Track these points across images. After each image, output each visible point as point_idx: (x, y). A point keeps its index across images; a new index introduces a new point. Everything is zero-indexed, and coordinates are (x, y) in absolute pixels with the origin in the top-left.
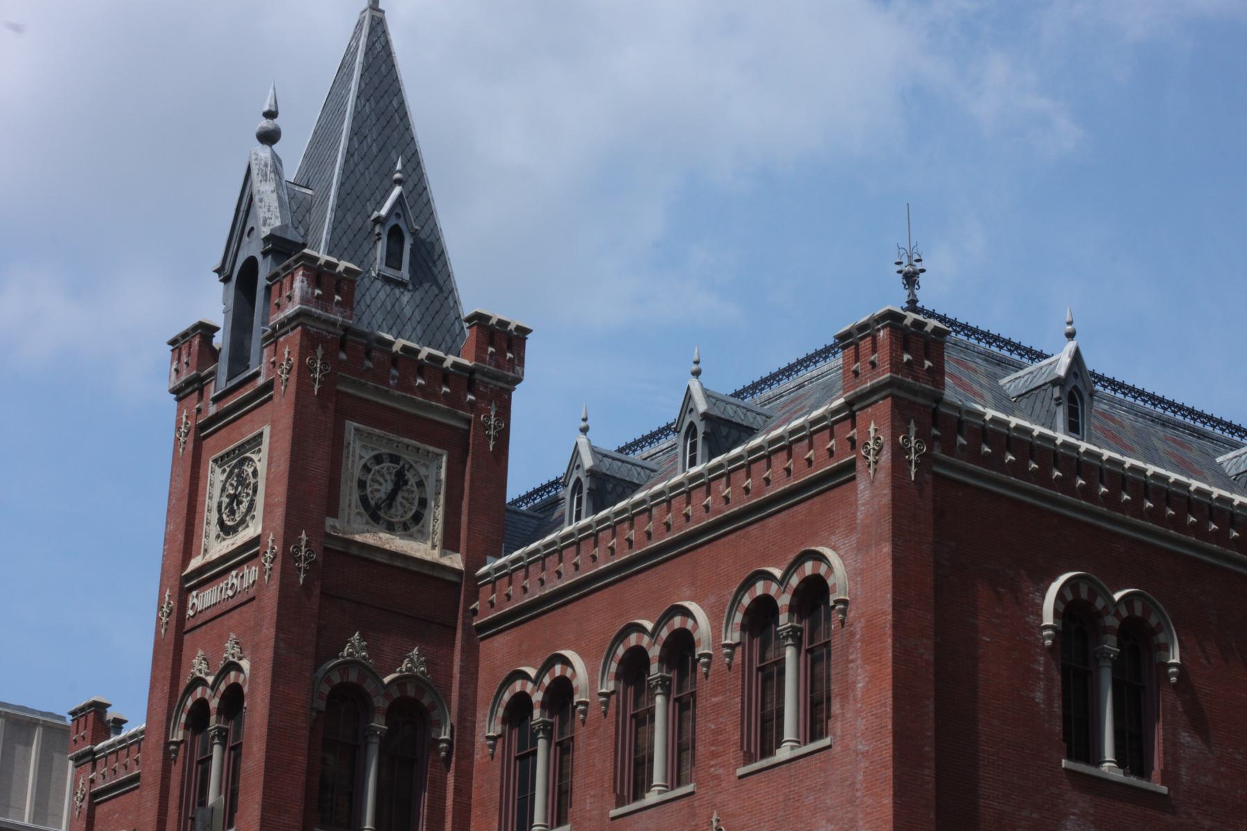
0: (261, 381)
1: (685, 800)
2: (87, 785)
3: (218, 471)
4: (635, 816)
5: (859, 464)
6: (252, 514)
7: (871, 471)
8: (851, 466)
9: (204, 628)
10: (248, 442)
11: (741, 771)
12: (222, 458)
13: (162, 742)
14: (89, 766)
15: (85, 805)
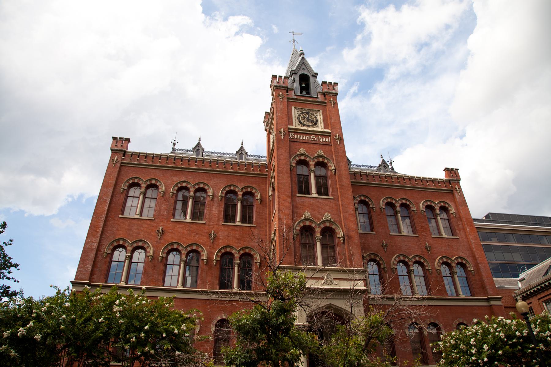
0: (319, 100)
1: (416, 238)
2: (120, 159)
3: (296, 111)
4: (399, 236)
5: (454, 191)
6: (317, 125)
7: (459, 194)
8: (452, 191)
9: (299, 143)
10: (313, 110)
11: (432, 236)
12: (299, 108)
13: (289, 165)
14: (122, 155)
15: (118, 165)
